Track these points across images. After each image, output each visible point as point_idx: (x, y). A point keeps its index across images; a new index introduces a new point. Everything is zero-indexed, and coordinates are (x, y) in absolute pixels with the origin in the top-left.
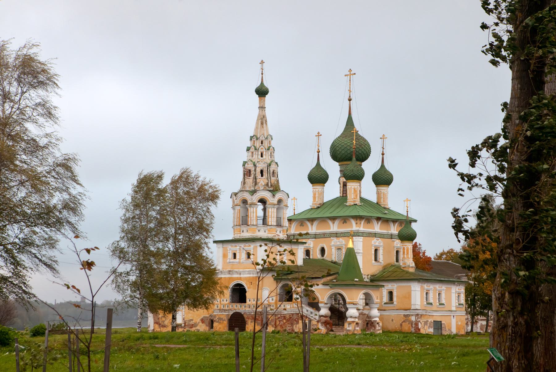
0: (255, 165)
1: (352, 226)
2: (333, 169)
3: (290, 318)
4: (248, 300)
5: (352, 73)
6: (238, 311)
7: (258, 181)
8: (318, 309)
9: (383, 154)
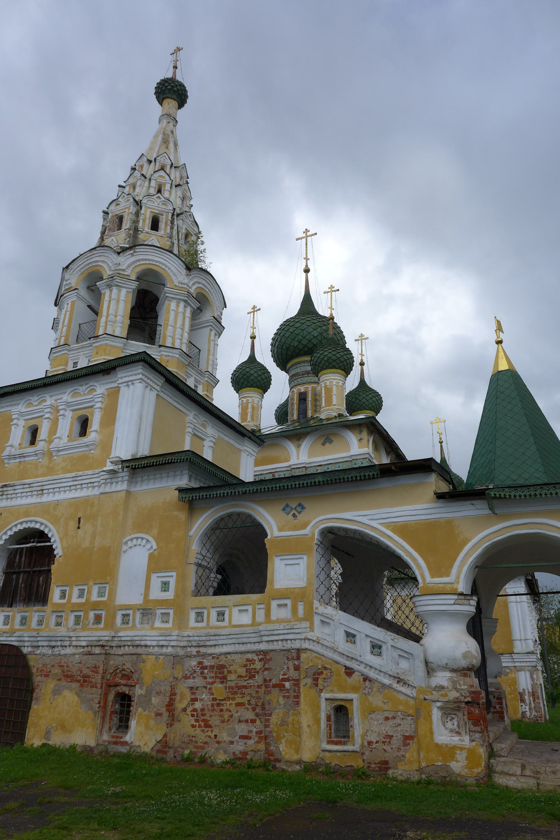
0: (138, 204)
1: (348, 447)
3: (251, 674)
4: (55, 595)
5: (308, 234)
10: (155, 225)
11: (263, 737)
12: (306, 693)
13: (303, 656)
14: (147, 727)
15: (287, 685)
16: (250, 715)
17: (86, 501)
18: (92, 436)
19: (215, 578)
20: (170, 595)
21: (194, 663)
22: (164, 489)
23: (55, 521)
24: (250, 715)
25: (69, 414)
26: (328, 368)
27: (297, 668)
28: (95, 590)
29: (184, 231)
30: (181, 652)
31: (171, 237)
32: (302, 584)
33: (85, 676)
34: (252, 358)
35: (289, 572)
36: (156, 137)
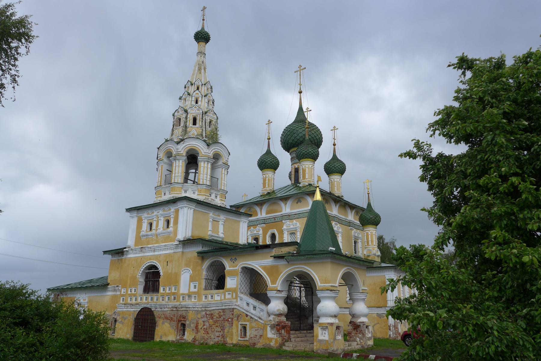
0: (186, 111)
2: (285, 158)
5: (301, 68)
6: (146, 306)
7: (188, 130)
8: (266, 301)
9: (334, 145)
10: (195, 123)
11: (223, 336)
12: (235, 322)
13: (235, 310)
14: (190, 334)
15: (230, 320)
16: (220, 330)
17: (169, 254)
18: (171, 229)
19: (215, 282)
20: (196, 290)
21: (204, 313)
22: (193, 251)
23: (160, 262)
24: (220, 330)
25: (162, 219)
26: (303, 158)
27: (233, 314)
28: (173, 288)
29: (209, 121)
30: (200, 309)
31: (202, 127)
32: (235, 286)
33: (171, 318)
34: (269, 152)
35: (231, 282)
36: (195, 67)
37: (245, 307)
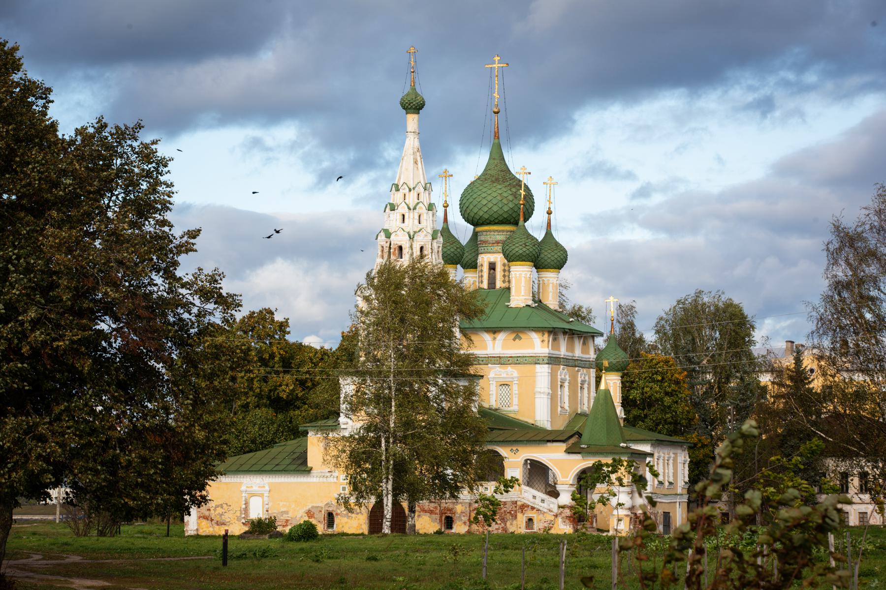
0: (411, 238)
1: (532, 346)
12: (519, 515)
37: (532, 500)
